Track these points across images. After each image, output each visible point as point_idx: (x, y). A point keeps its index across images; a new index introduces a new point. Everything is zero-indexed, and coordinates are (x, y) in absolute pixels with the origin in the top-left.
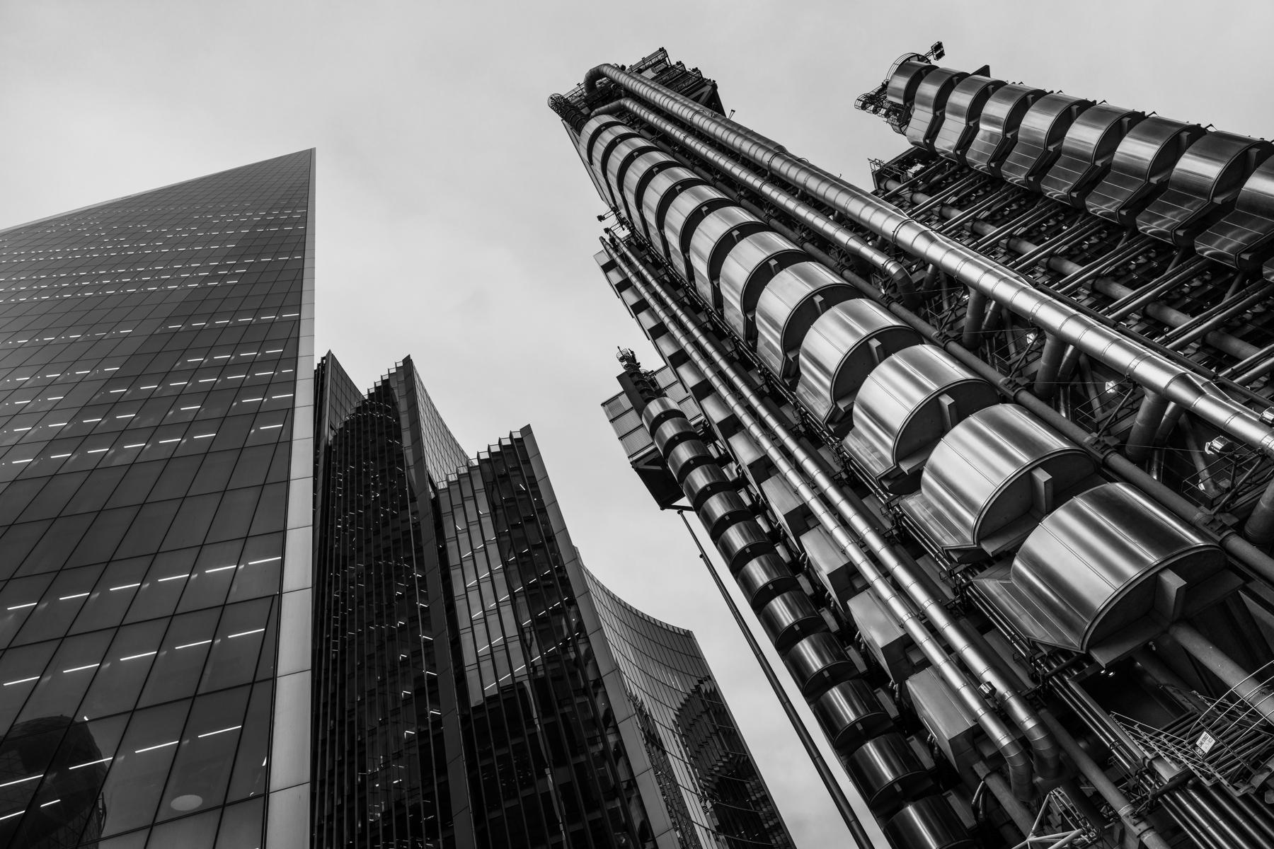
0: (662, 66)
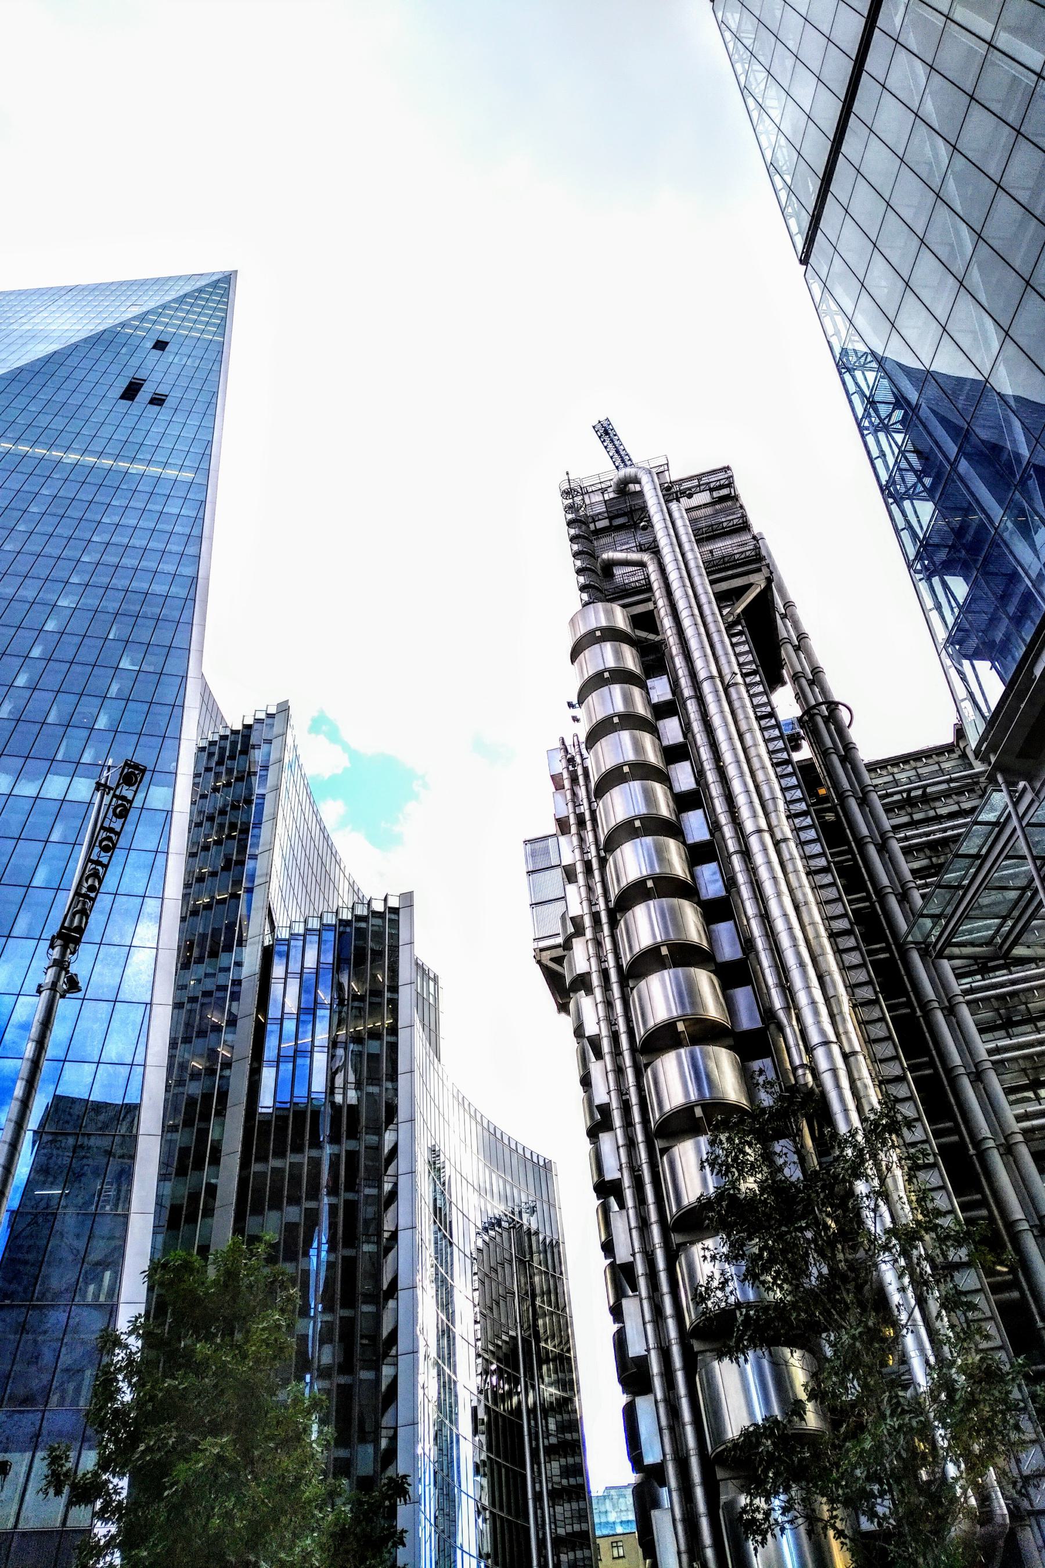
0: (725, 492)
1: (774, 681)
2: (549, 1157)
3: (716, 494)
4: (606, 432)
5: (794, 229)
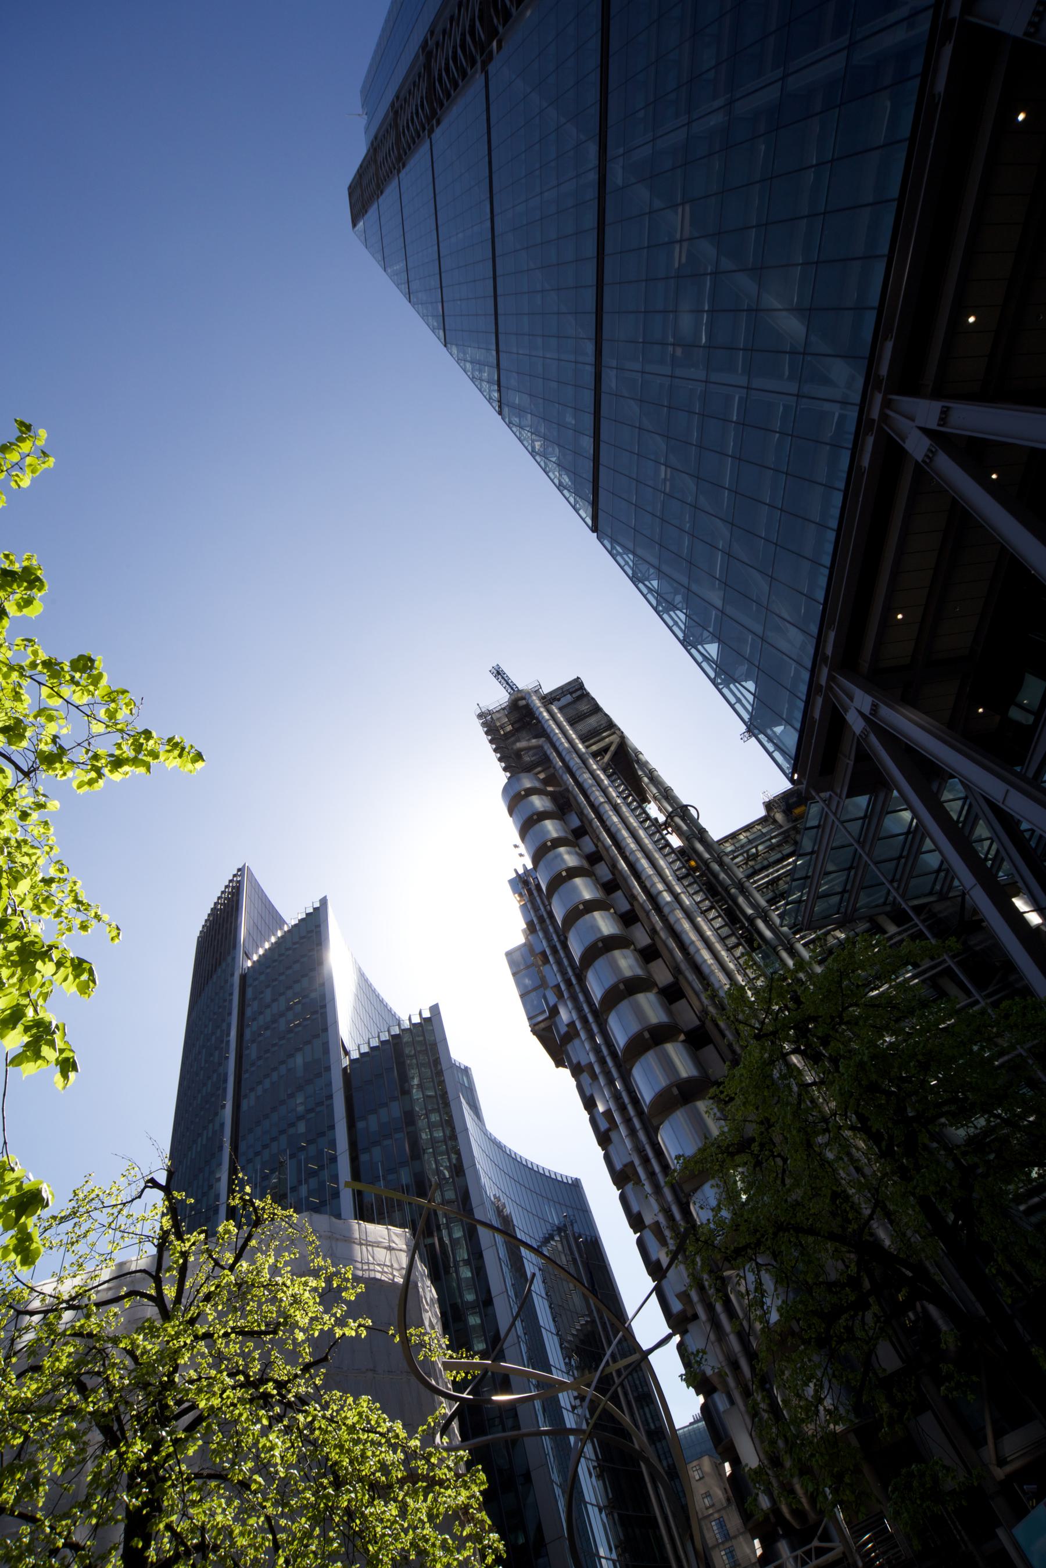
0: (579, 693)
1: (643, 799)
2: (574, 1176)
3: (574, 695)
4: (499, 673)
5: (584, 515)
